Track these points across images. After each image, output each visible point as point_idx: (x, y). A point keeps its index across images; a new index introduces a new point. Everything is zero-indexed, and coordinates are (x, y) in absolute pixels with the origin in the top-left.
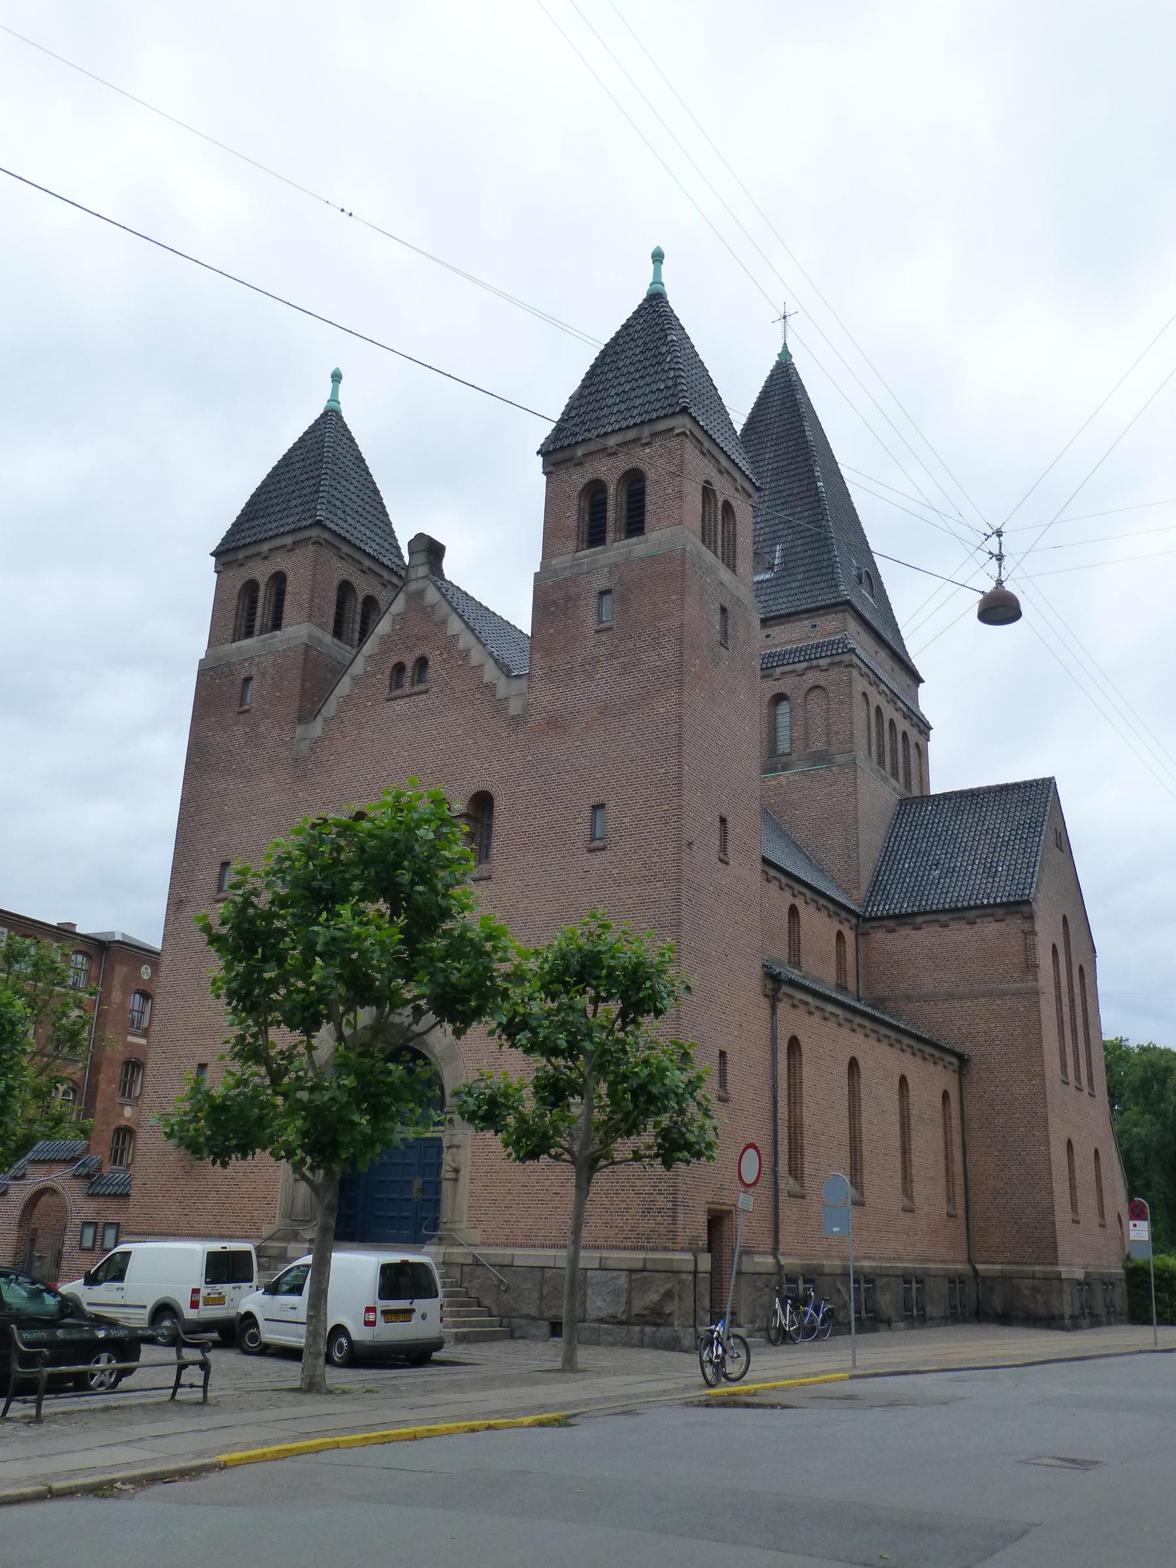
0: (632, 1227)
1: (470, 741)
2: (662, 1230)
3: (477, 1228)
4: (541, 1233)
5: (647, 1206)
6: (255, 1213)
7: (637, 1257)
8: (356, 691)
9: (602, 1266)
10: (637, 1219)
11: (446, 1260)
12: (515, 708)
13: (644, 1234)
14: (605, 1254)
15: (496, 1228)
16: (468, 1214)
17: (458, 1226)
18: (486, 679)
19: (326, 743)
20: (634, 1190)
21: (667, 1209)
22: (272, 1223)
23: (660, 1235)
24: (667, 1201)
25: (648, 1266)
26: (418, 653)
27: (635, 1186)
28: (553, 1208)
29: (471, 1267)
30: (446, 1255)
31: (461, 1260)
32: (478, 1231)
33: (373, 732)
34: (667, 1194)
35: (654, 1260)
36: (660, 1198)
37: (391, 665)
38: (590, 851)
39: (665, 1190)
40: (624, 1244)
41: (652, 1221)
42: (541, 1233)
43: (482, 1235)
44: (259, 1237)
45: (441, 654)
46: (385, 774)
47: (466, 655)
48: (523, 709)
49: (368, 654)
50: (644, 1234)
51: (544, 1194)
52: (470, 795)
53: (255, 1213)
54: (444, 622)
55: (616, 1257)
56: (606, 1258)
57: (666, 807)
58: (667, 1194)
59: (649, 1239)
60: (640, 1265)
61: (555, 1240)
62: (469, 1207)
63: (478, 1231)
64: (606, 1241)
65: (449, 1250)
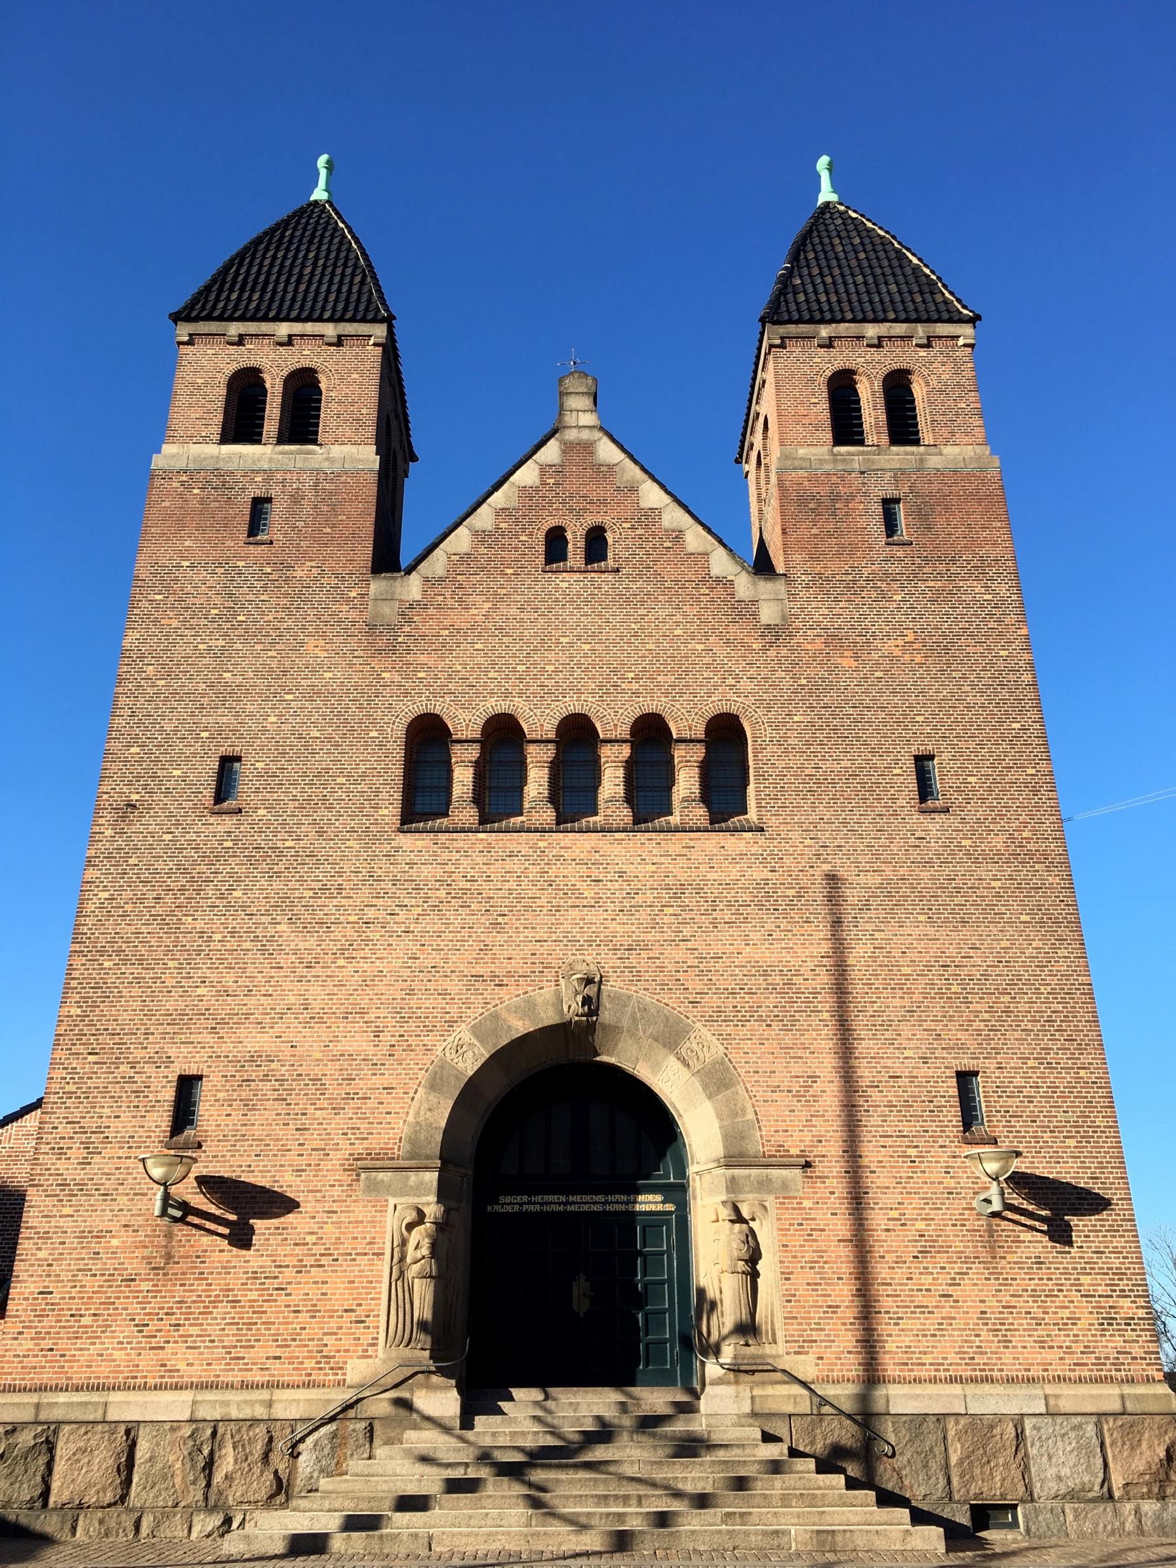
0: (1085, 1347)
1: (700, 647)
2: (1137, 1351)
3: (807, 1353)
4: (927, 1359)
5: (1104, 1315)
6: (330, 1340)
7: (1107, 1397)
8: (483, 550)
9: (1052, 1411)
10: (1093, 1335)
11: (757, 1409)
12: (768, 614)
13: (1108, 1358)
14: (1050, 1389)
15: (843, 1352)
16: (786, 1330)
17: (768, 1349)
18: (716, 571)
19: (431, 611)
20: (1079, 1291)
21: (1139, 1319)
22: (370, 1357)
23: (1134, 1358)
24: (1137, 1307)
25: (1130, 1407)
26: (591, 520)
27: (1080, 1285)
28: (943, 1318)
29: (809, 1418)
30: (757, 1400)
31: (789, 1408)
32: (811, 1357)
33: (522, 610)
34: (1135, 1296)
35: (1138, 1398)
36: (1125, 1303)
37: (546, 527)
38: (923, 812)
39: (1130, 1291)
40: (1077, 1373)
41: (1117, 1338)
42: (927, 1359)
43: (817, 1365)
44: (340, 1384)
45: (633, 528)
46: (550, 668)
47: (678, 536)
48: (783, 618)
49: (500, 506)
50: (1108, 1358)
51: (923, 1296)
52: (709, 716)
53: (330, 1340)
54: (633, 489)
55: (1072, 1397)
56: (1057, 1397)
57: (1031, 771)
58: (1135, 1296)
59: (1118, 1366)
60: (1116, 1406)
61: (954, 1370)
62: (785, 1318)
63: (811, 1357)
64: (1047, 1370)
65: (757, 1392)
